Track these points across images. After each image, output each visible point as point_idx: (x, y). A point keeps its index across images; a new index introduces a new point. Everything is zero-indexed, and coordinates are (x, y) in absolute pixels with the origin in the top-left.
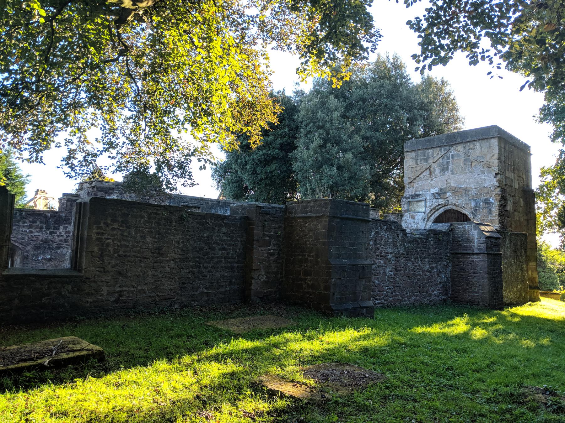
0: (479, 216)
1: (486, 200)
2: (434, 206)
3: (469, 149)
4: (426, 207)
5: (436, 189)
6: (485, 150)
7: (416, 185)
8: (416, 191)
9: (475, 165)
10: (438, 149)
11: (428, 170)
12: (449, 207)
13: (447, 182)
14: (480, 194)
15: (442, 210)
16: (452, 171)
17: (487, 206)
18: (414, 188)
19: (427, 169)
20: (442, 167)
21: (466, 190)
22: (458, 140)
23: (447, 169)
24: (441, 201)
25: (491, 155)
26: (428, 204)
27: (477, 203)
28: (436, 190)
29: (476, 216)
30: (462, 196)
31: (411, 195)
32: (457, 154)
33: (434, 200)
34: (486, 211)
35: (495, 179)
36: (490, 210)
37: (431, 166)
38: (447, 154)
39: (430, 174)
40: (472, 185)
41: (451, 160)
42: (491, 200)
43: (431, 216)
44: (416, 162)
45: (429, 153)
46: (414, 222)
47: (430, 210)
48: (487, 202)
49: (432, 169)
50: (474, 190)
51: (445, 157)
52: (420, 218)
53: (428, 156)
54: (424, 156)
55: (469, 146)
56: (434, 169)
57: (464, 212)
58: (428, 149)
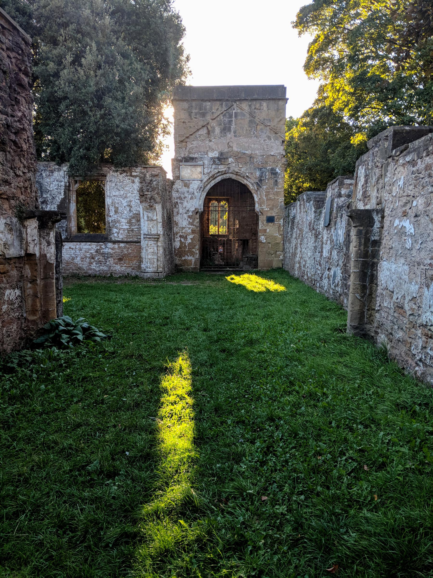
0: (265, 187)
1: (272, 169)
2: (213, 173)
3: (255, 109)
4: (204, 174)
5: (216, 152)
6: (272, 113)
7: (189, 146)
8: (190, 153)
9: (261, 129)
10: (218, 103)
11: (205, 128)
12: (228, 175)
13: (229, 147)
14: (266, 163)
15: (219, 179)
16: (235, 132)
17: (273, 176)
18: (188, 149)
19: (203, 126)
20: (223, 126)
21: (251, 157)
22: (243, 96)
23: (229, 130)
24: (222, 168)
25: (279, 119)
26: (206, 171)
27: (262, 173)
28: (215, 154)
29: (261, 187)
30: (246, 163)
31: (184, 158)
32: (241, 112)
33: (214, 166)
34: (272, 182)
35: (282, 148)
36: (276, 181)
37: (208, 124)
38: (229, 111)
39: (209, 133)
40: (257, 152)
41: (233, 119)
42: (277, 170)
43: (207, 185)
44: (190, 115)
45: (206, 106)
46: (188, 192)
47: (208, 178)
48: (273, 173)
49: (209, 127)
50: (260, 158)
51: (227, 114)
52: (196, 187)
53: (206, 109)
54: (200, 109)
55: (255, 106)
56: (213, 128)
57: (245, 182)
58: (206, 101)
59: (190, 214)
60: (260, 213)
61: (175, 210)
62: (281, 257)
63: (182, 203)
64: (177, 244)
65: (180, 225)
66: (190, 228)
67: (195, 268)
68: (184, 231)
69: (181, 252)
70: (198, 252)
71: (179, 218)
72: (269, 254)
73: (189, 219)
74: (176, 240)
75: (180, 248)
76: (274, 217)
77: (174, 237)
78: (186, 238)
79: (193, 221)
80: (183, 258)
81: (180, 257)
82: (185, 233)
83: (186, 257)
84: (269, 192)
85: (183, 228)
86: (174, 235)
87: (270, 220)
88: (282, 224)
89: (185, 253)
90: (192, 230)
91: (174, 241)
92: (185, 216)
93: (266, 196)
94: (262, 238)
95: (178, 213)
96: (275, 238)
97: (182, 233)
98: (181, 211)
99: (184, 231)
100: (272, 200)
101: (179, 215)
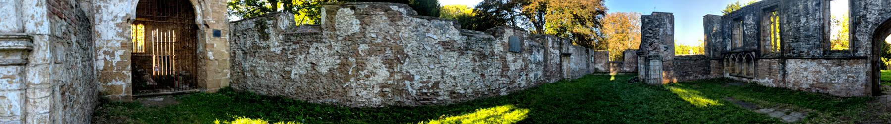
59: (119, 21)
60: (204, 26)
61: (97, 16)
62: (228, 75)
63: (107, 7)
64: (100, 64)
65: (104, 37)
66: (119, 40)
67: (126, 97)
68: (109, 45)
69: (106, 75)
70: (130, 74)
71: (103, 28)
72: (217, 72)
73: (117, 28)
74: (99, 58)
75: (105, 69)
76: (220, 31)
77: (96, 53)
78: (113, 55)
79: (123, 32)
80: (110, 84)
81: (105, 82)
82: (111, 48)
83: (114, 82)
84: (214, 4)
85: (109, 41)
86: (95, 51)
87: (217, 34)
88: (228, 40)
89: (113, 77)
90: (122, 44)
91: (96, 60)
92: (112, 24)
93: (212, 7)
94: (210, 55)
95: (101, 20)
96: (222, 54)
97: (107, 47)
98: (105, 17)
99: (109, 45)
100: (217, 13)
101: (103, 23)
